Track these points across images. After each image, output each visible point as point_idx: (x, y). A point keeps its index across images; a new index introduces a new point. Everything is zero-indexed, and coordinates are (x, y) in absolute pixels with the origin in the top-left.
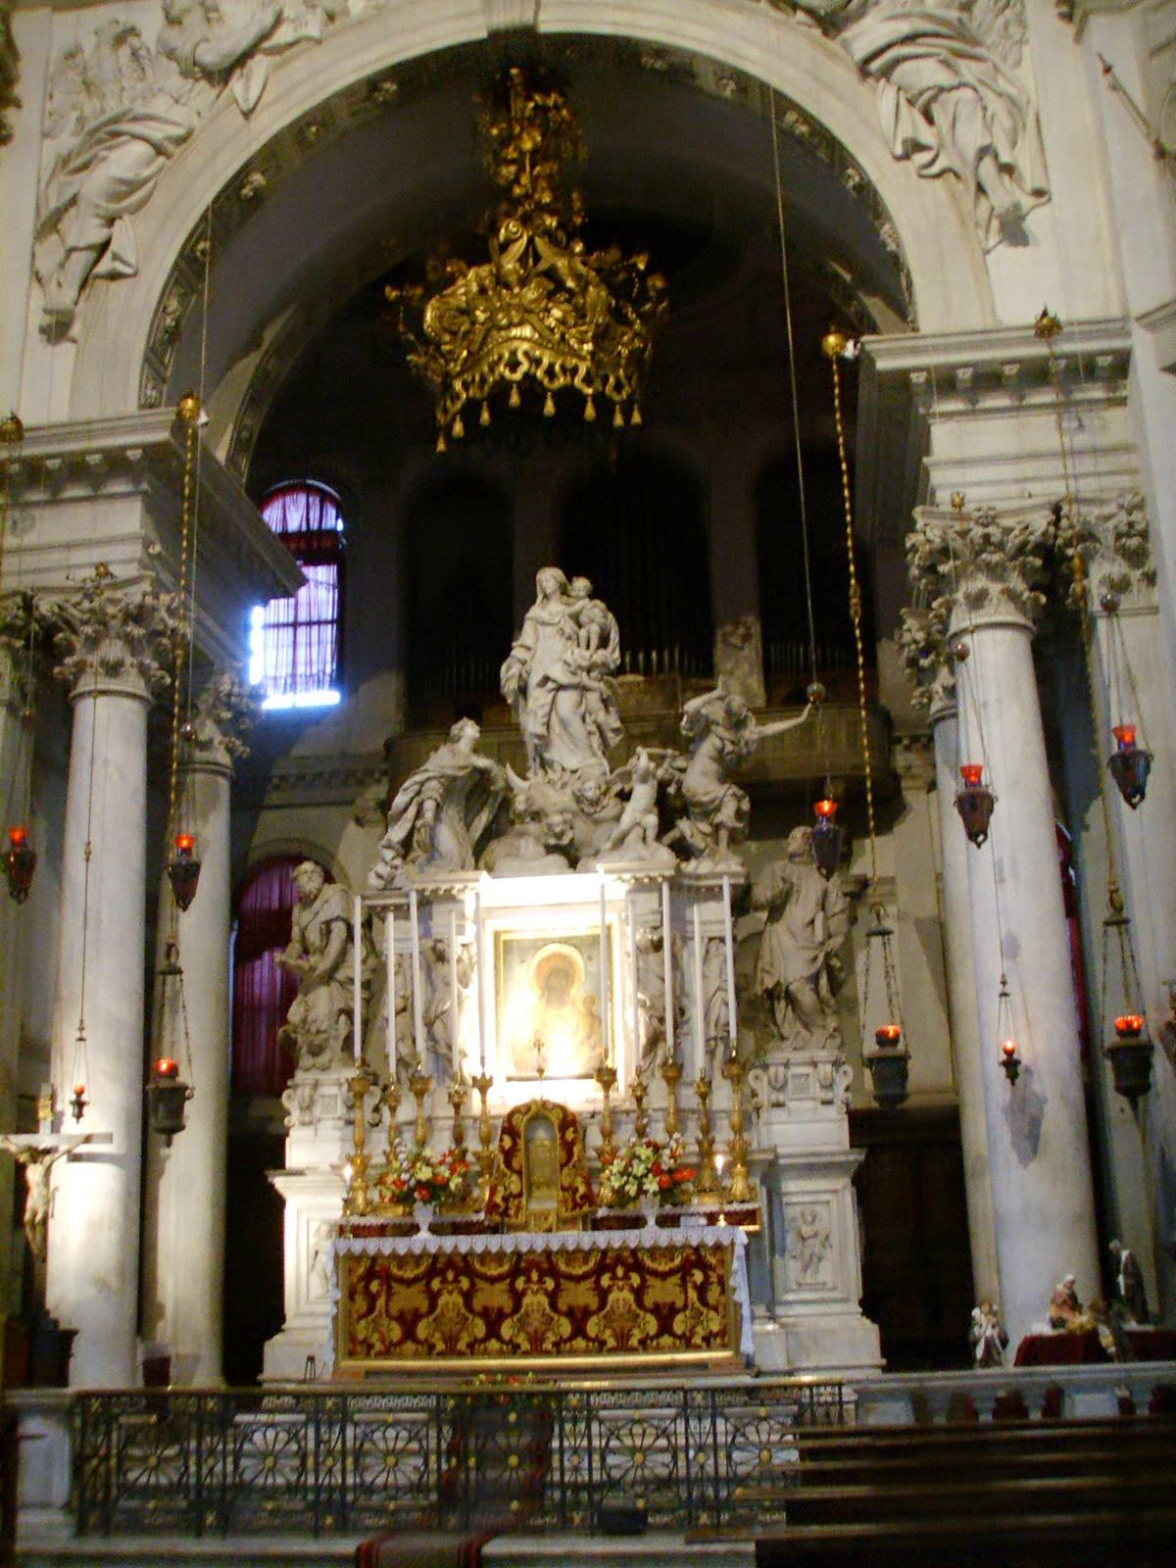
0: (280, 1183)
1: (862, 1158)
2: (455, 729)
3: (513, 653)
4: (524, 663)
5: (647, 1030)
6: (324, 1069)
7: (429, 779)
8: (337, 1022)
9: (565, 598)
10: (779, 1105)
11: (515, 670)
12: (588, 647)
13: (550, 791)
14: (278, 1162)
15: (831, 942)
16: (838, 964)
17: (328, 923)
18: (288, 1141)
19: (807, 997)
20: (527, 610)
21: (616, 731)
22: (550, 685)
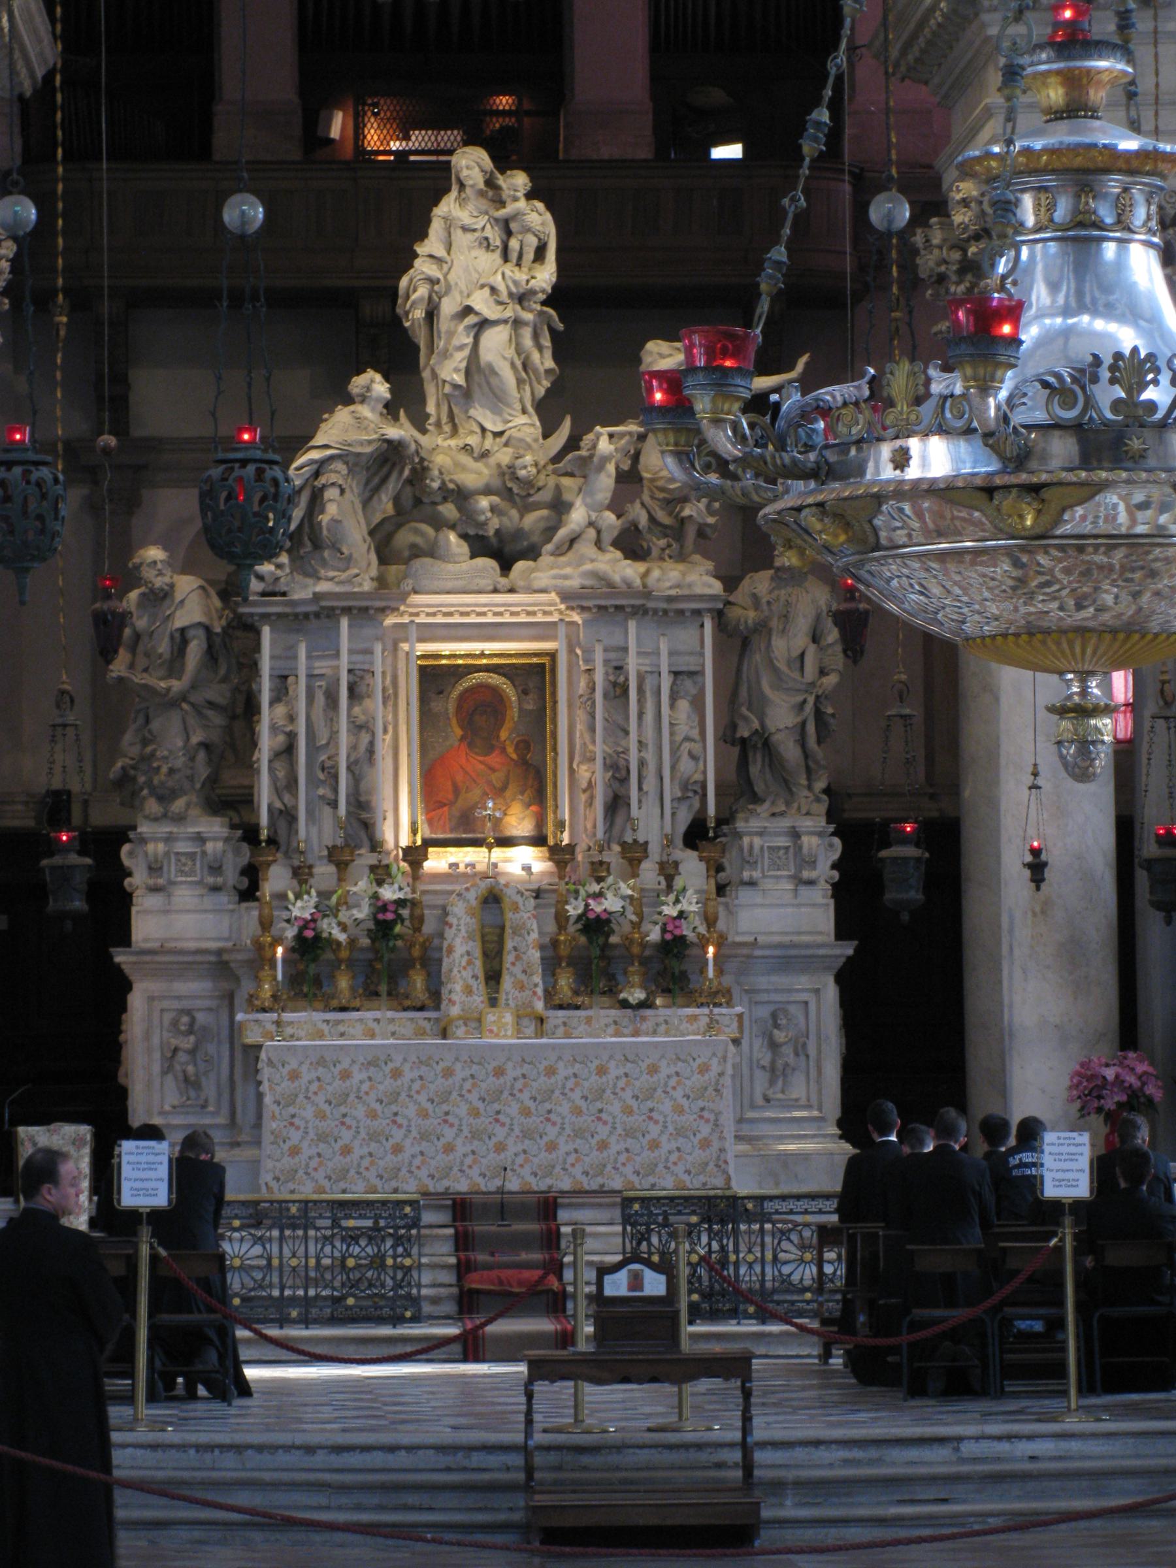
0: (121, 957)
1: (850, 952)
2: (358, 383)
3: (417, 263)
4: (433, 282)
5: (605, 794)
6: (180, 819)
7: (331, 458)
8: (192, 759)
9: (490, 193)
10: (752, 883)
11: (422, 291)
12: (519, 265)
13: (465, 459)
14: (125, 940)
15: (825, 680)
16: (830, 711)
17: (183, 631)
18: (134, 910)
19: (790, 751)
20: (436, 203)
21: (548, 372)
22: (471, 320)
